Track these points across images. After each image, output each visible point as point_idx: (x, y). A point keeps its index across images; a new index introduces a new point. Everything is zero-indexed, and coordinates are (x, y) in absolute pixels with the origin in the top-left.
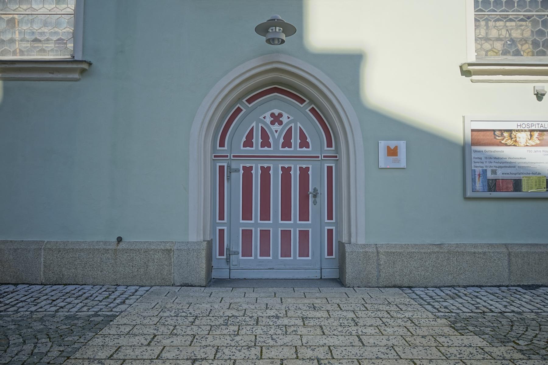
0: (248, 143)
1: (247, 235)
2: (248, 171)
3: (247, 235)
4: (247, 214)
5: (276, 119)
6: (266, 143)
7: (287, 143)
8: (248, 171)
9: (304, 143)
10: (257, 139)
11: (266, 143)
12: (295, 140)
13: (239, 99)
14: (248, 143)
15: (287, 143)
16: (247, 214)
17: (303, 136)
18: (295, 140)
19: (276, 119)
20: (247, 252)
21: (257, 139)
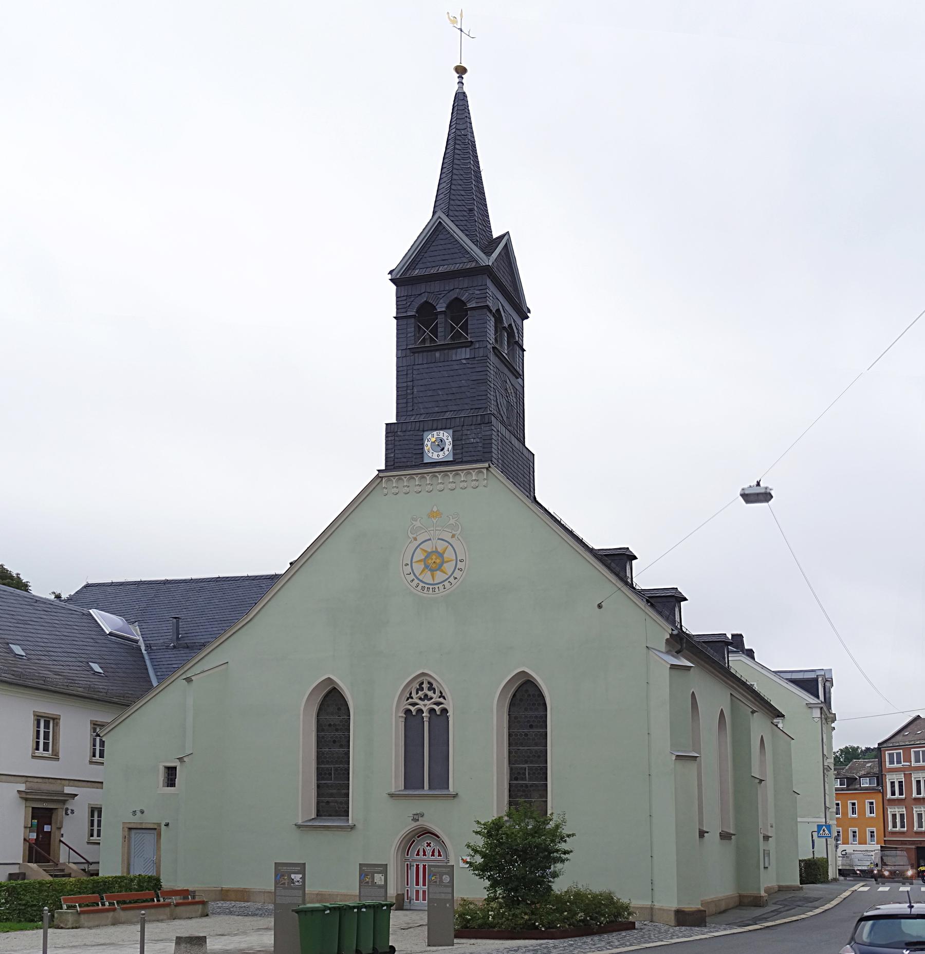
0: (418, 854)
1: (417, 892)
2: (417, 866)
3: (417, 892)
4: (417, 884)
5: (429, 845)
6: (425, 854)
7: (433, 855)
8: (417, 866)
9: (440, 855)
10: (421, 853)
11: (425, 854)
12: (436, 853)
13: (414, 837)
14: (418, 854)
15: (433, 855)
16: (417, 884)
17: (439, 852)
18: (436, 853)
19: (429, 845)
20: (417, 899)
21: (421, 853)
